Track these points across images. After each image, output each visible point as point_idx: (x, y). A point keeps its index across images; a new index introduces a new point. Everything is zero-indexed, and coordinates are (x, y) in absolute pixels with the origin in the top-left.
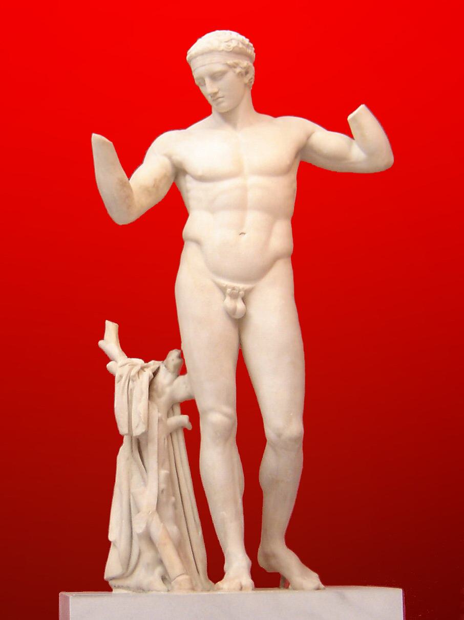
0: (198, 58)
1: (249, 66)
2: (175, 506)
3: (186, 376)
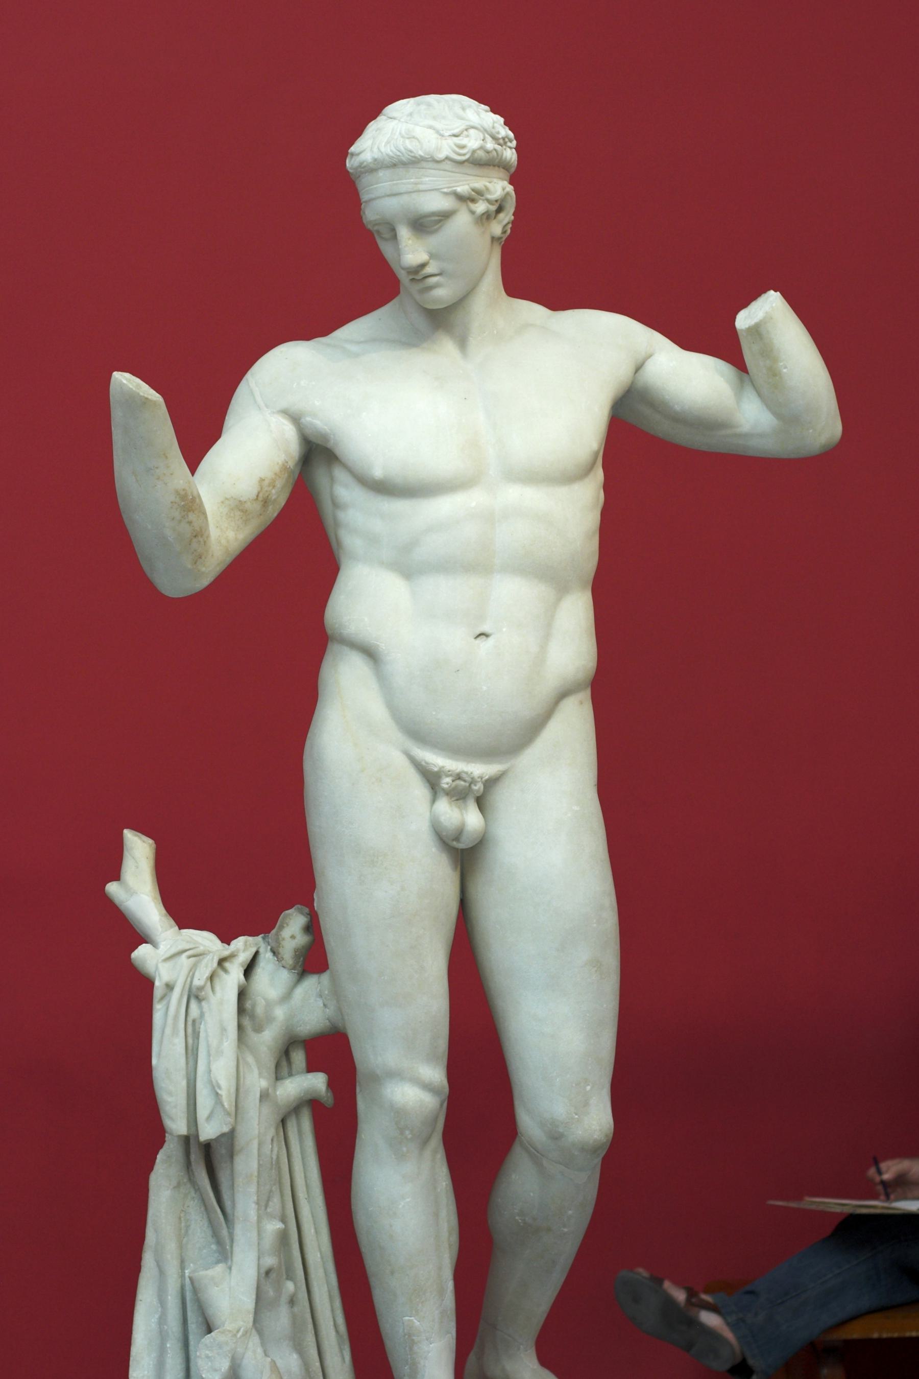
0: (381, 174)
1: (508, 194)
2: (292, 1302)
3: (325, 977)
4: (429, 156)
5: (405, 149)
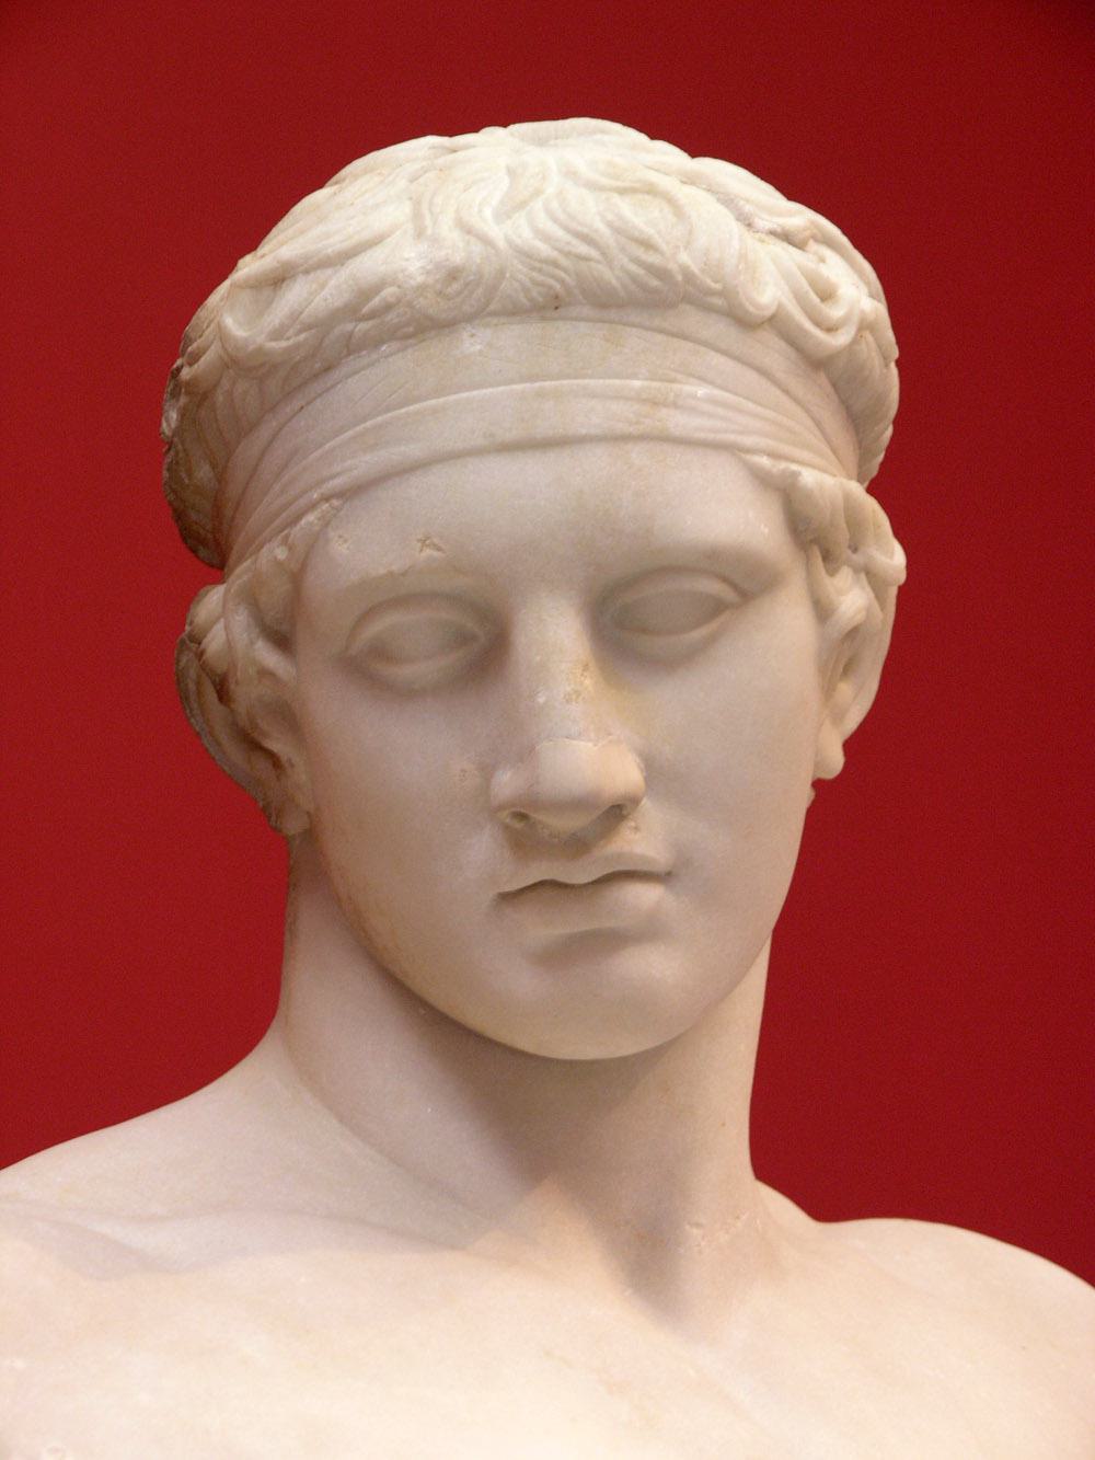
0: (472, 343)
4: (718, 286)
5: (617, 231)
